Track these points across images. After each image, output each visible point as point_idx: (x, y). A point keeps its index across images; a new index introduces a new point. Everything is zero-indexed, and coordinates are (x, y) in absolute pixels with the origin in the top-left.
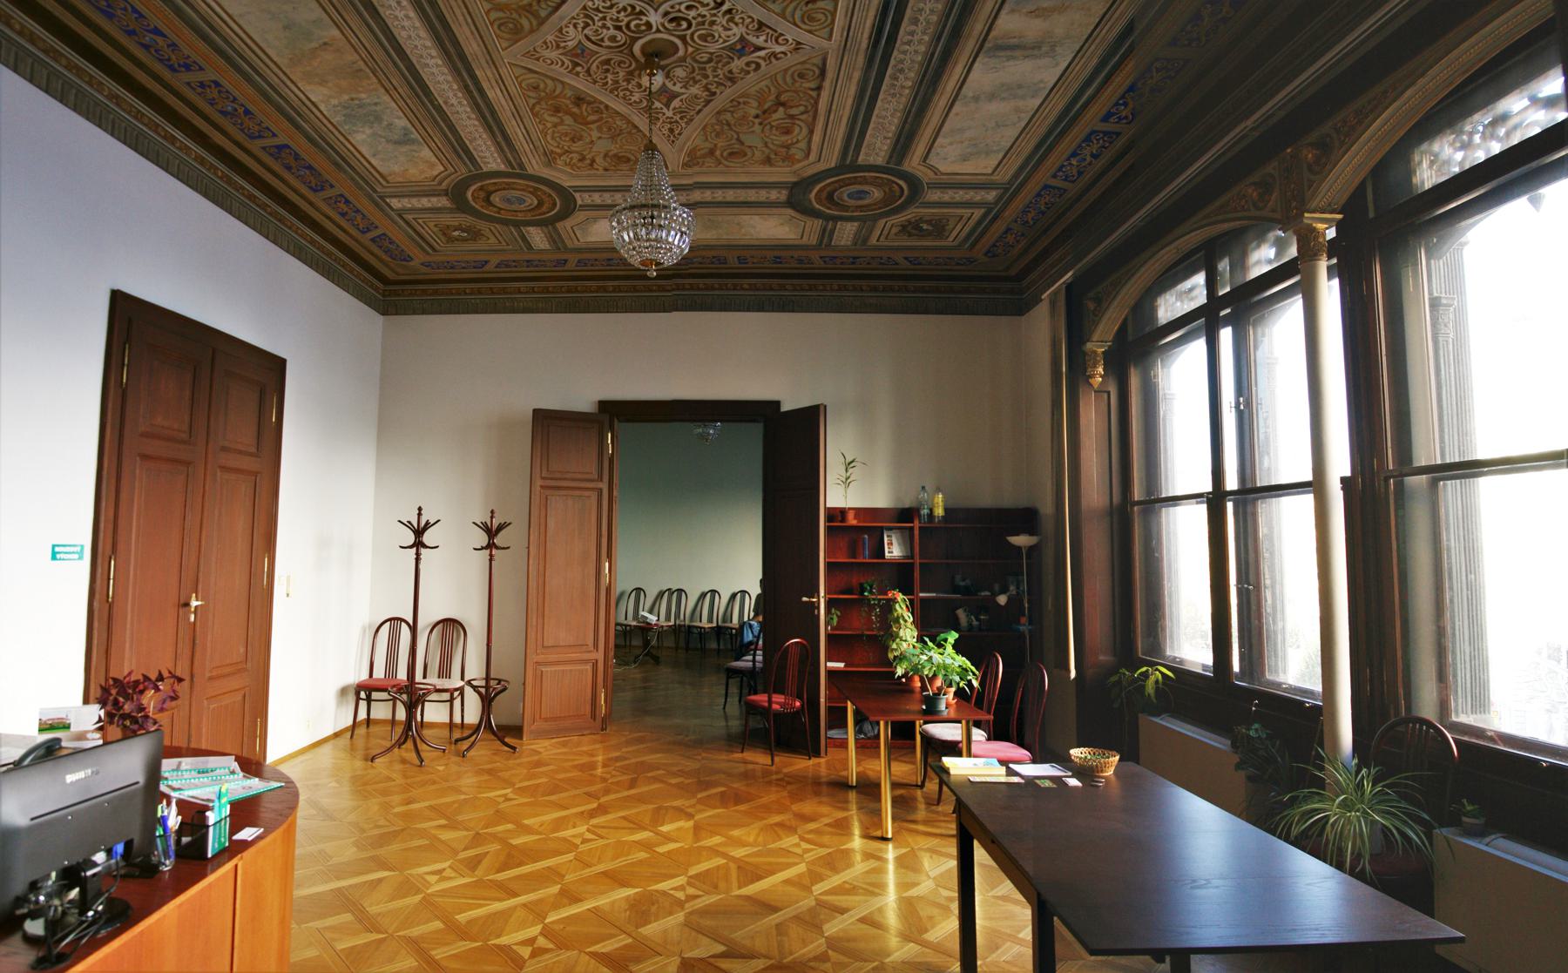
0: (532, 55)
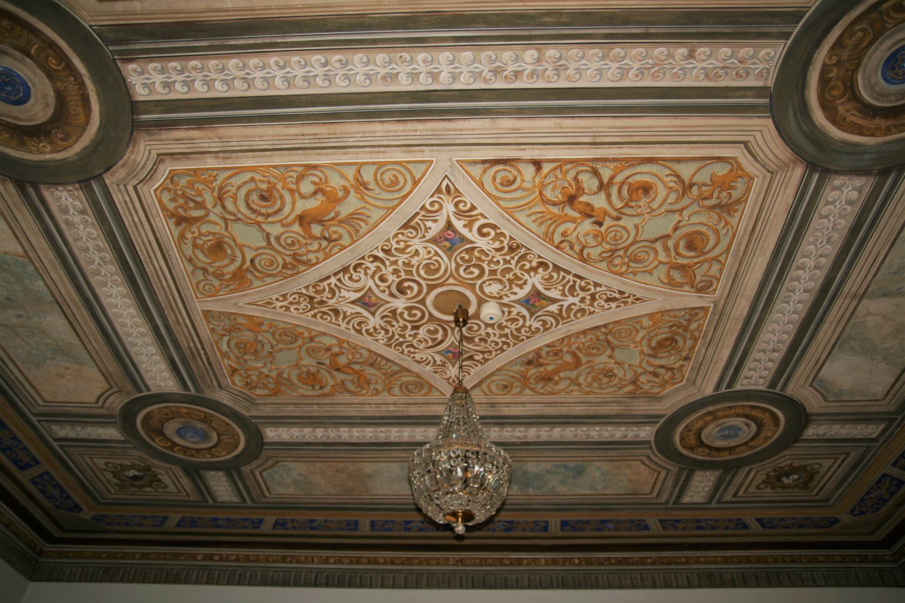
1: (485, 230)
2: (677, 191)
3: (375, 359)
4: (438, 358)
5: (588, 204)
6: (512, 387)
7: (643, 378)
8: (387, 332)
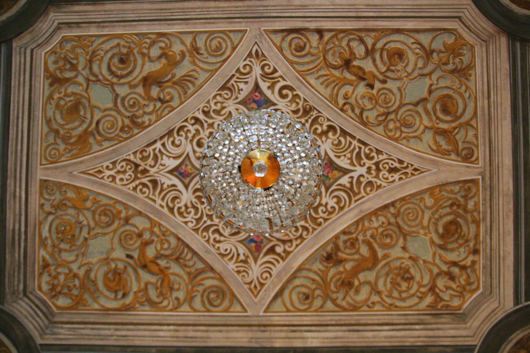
0: (256, 287)
1: (285, 92)
2: (422, 57)
3: (182, 252)
4: (242, 249)
5: (360, 68)
6: (314, 298)
7: (441, 283)
8: (196, 209)
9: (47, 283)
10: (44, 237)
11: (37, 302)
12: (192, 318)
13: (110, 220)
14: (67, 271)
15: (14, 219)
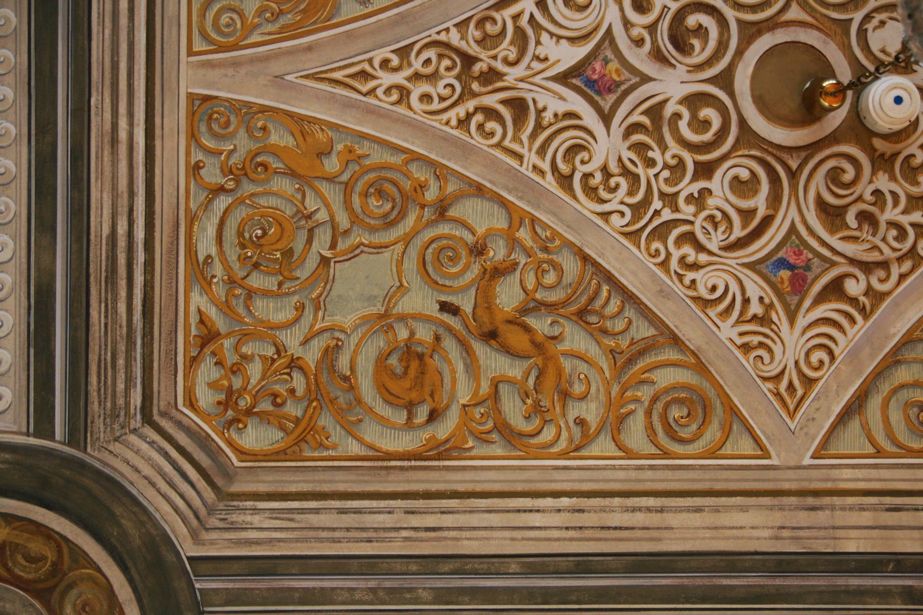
3: (594, 295)
4: (755, 287)
8: (634, 179)
9: (212, 385)
10: (201, 258)
11: (183, 439)
12: (621, 475)
13: (393, 208)
14: (270, 351)
15: (114, 207)
